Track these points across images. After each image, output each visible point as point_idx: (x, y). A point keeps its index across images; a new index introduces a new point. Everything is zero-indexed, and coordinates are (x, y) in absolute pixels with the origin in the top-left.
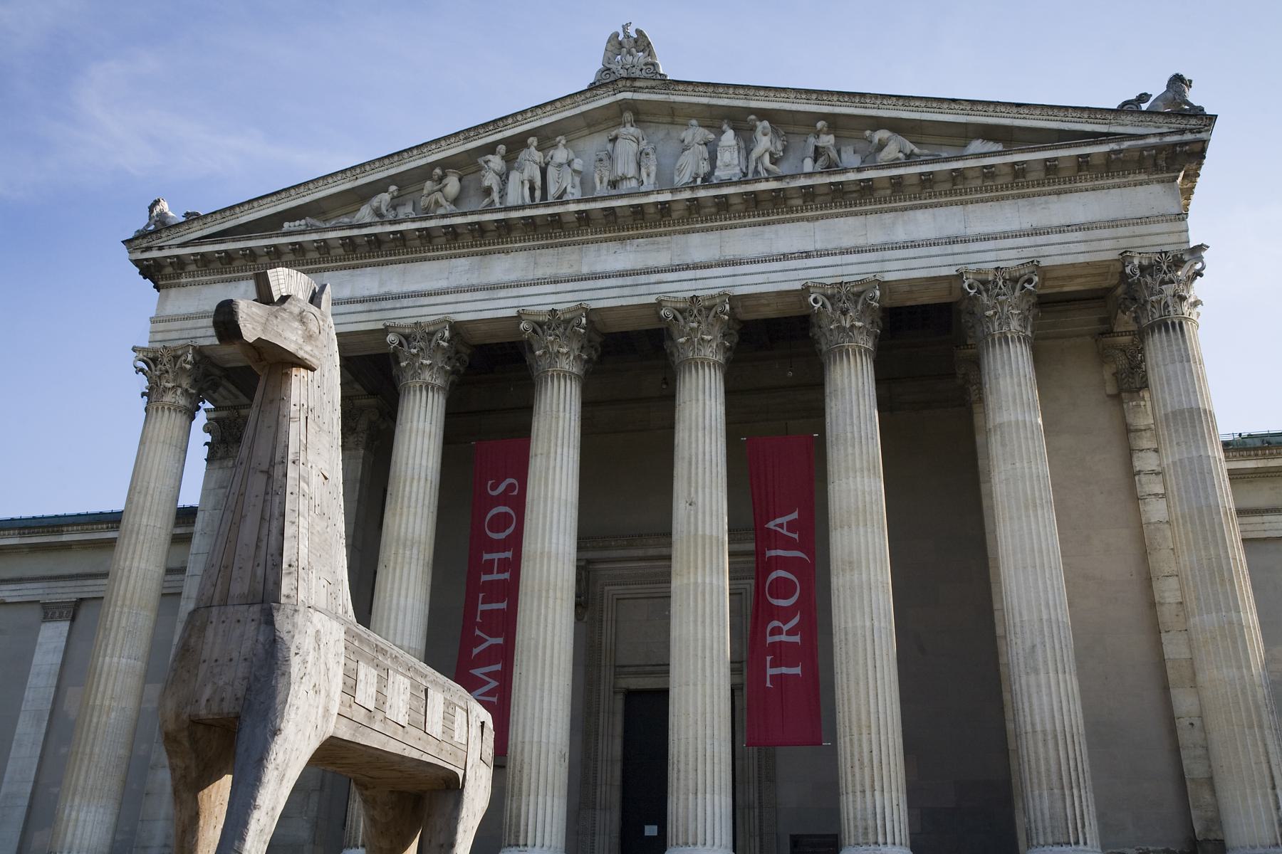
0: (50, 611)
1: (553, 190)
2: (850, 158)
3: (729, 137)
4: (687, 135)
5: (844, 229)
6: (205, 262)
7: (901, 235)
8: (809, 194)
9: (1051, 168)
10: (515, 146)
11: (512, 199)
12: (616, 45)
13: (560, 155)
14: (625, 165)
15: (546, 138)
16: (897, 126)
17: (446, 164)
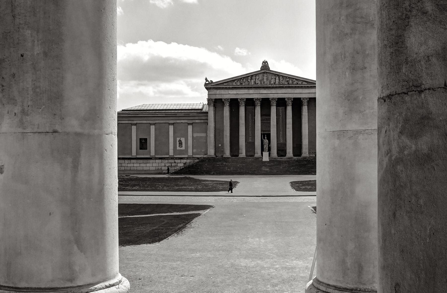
0: (189, 124)
1: (257, 83)
2: (291, 82)
3: (277, 78)
4: (273, 77)
5: (289, 90)
6: (214, 88)
7: (295, 92)
8: (286, 87)
9: (311, 87)
10: (252, 76)
11: (252, 84)
12: (263, 62)
13: (257, 77)
14: (265, 80)
15: (256, 75)
16: (296, 79)
17: (244, 78)
